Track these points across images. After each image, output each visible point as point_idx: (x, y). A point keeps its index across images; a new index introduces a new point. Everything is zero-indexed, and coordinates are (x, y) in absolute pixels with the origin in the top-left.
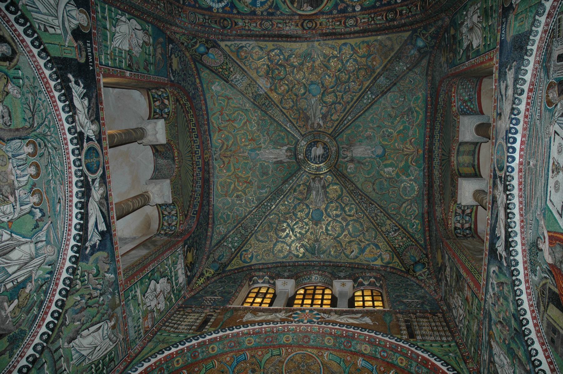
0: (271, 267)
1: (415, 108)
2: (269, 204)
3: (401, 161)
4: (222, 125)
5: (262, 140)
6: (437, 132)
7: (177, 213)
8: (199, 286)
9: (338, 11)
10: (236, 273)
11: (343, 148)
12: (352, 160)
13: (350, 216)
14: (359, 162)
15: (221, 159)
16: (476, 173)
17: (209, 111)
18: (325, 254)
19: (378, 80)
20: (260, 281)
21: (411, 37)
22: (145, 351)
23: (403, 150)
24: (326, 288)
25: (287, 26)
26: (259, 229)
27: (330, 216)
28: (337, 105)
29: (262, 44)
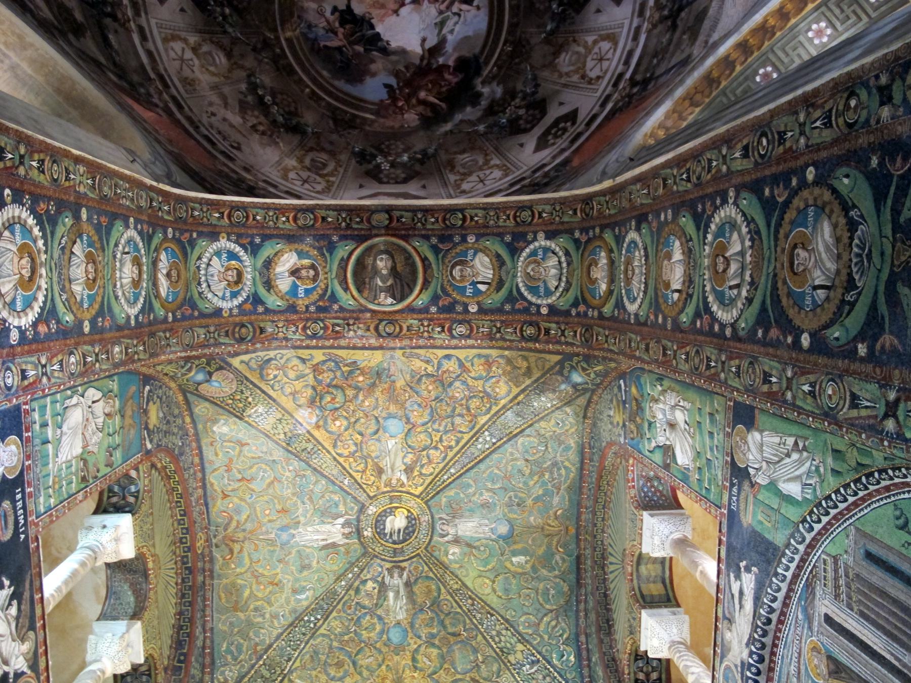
1: (563, 462)
2: (312, 619)
3: (540, 546)
4: (230, 488)
5: (300, 510)
6: (601, 507)
7: (149, 670)
9: (439, 308)
11: (441, 519)
12: (457, 541)
13: (454, 634)
15: (227, 545)
16: (668, 595)
17: (207, 465)
19: (503, 417)
21: (561, 363)
23: (543, 528)
25: (349, 330)
27: (419, 637)
28: (432, 452)
29: (304, 353)
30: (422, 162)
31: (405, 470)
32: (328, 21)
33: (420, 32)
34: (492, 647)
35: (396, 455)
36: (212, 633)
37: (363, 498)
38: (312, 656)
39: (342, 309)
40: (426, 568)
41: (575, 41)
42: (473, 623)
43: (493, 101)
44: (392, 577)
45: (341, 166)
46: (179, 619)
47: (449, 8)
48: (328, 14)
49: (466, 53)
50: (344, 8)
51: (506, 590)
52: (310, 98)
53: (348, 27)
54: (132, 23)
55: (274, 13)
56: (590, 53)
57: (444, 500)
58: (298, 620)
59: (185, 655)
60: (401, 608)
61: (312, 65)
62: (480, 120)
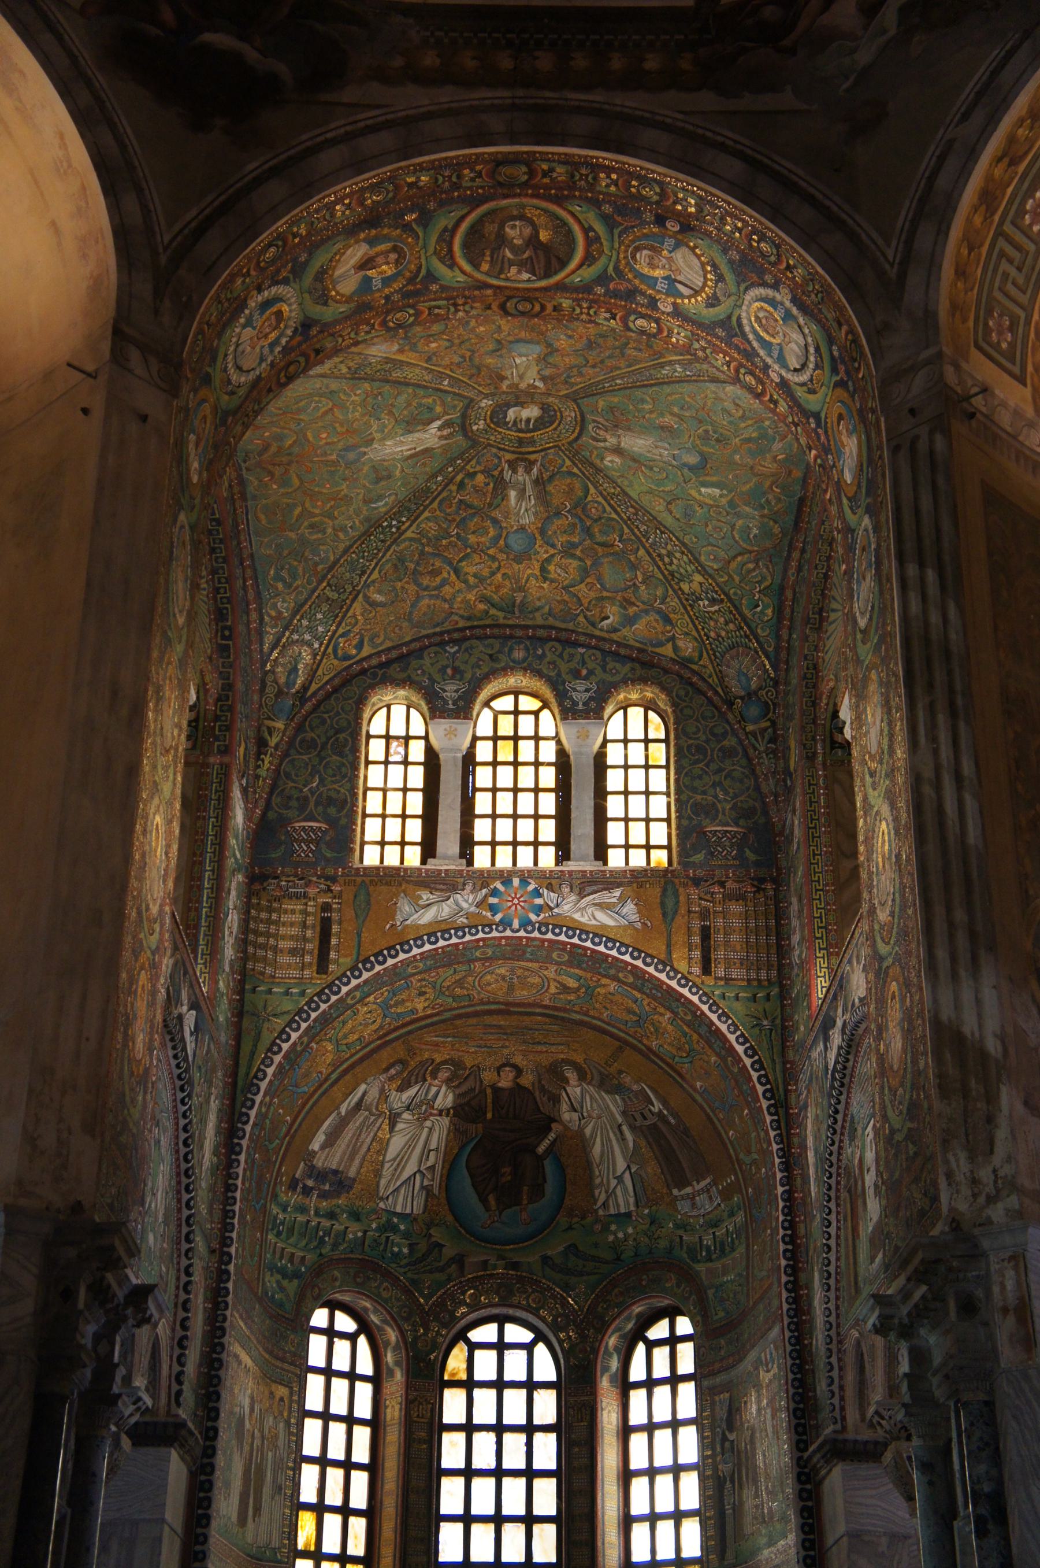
0: (409, 654)
5: (375, 427)
8: (264, 780)
9: (607, 291)
10: (328, 696)
11: (594, 421)
12: (618, 451)
13: (603, 545)
14: (636, 461)
18: (537, 615)
20: (387, 699)
22: (246, 1048)
23: (752, 468)
24: (545, 705)
25: (457, 311)
26: (373, 577)
27: (553, 546)
28: (584, 370)
31: (543, 379)
34: (659, 568)
35: (527, 368)
36: (253, 560)
37: (471, 394)
38: (395, 566)
39: (443, 288)
40: (568, 463)
42: (634, 534)
44: (515, 471)
46: (213, 580)
51: (686, 514)
57: (601, 404)
58: (373, 525)
59: (230, 628)
60: (526, 510)
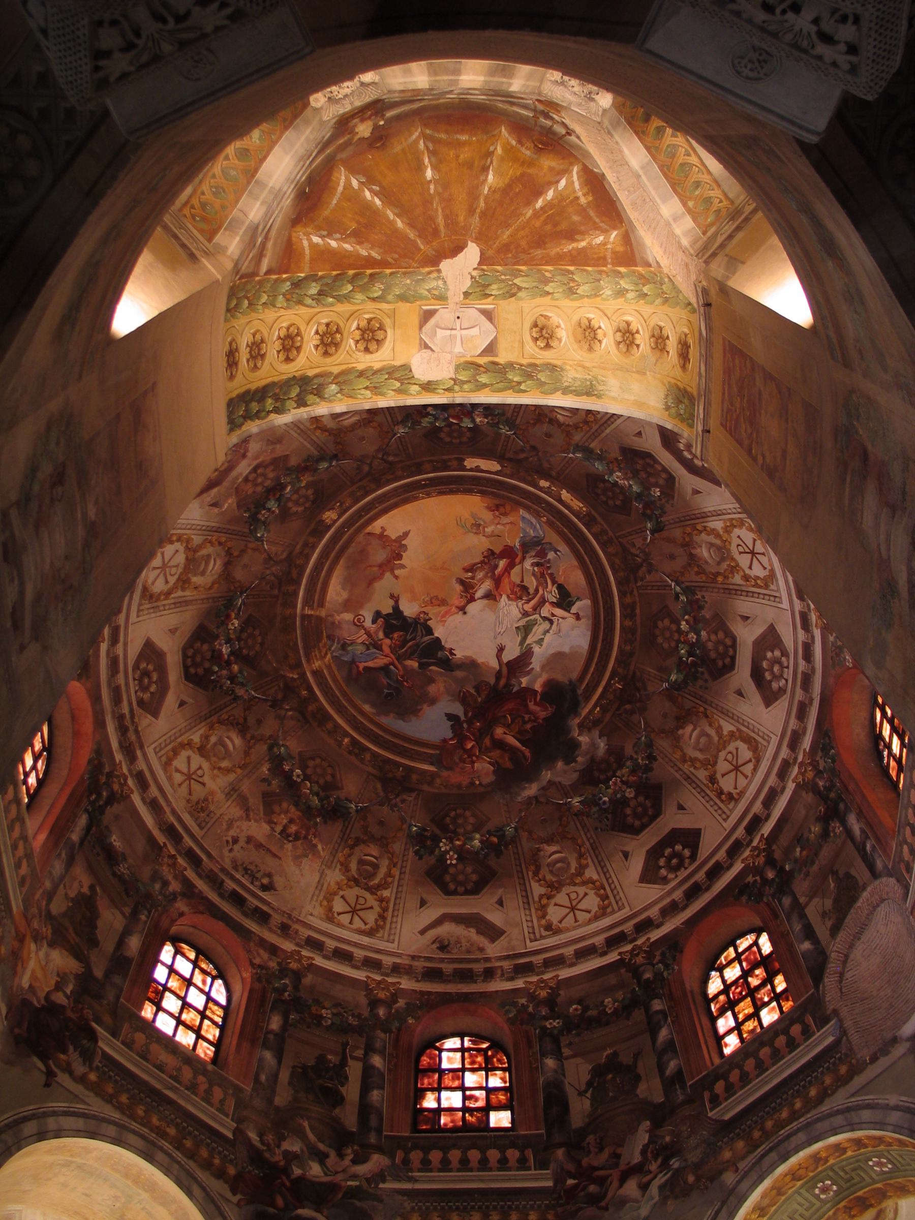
30: (497, 850)
32: (368, 633)
33: (495, 638)
41: (707, 717)
43: (593, 760)
45: (395, 865)
47: (535, 609)
48: (368, 623)
49: (559, 677)
50: (391, 611)
52: (350, 752)
53: (395, 635)
54: (130, 782)
55: (296, 644)
56: (724, 748)
61: (350, 701)
62: (575, 789)
